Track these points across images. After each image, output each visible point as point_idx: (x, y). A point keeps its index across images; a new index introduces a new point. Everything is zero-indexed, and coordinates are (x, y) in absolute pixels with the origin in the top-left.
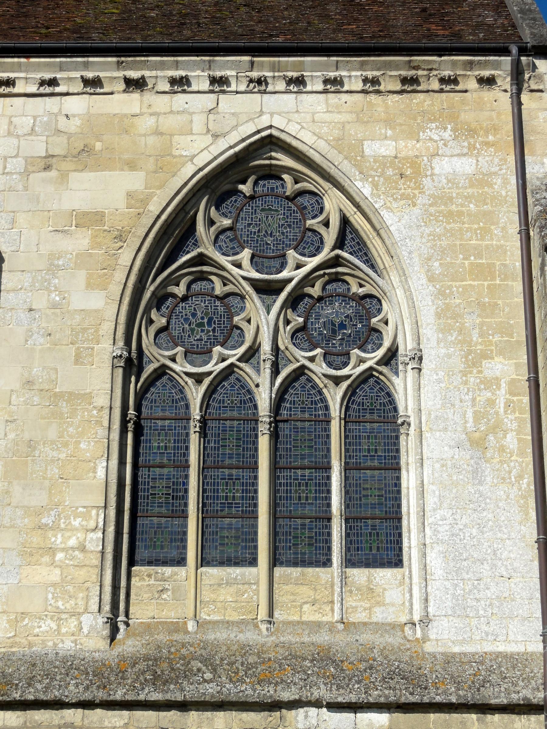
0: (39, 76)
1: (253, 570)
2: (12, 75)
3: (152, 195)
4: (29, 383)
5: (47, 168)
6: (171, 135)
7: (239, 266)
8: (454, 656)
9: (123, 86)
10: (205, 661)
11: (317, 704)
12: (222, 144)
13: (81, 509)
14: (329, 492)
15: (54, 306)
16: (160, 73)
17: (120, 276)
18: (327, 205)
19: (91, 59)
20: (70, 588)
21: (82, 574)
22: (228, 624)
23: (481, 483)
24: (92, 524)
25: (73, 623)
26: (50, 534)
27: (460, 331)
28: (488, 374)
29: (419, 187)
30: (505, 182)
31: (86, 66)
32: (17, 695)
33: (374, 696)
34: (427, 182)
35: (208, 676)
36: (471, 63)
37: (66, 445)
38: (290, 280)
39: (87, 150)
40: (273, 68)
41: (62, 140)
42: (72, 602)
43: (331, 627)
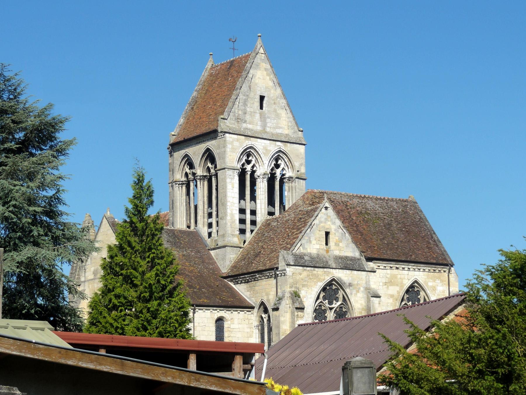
5: (385, 285)
18: (421, 293)
29: (435, 292)
30: (447, 292)
34: (436, 291)
41: (387, 279)
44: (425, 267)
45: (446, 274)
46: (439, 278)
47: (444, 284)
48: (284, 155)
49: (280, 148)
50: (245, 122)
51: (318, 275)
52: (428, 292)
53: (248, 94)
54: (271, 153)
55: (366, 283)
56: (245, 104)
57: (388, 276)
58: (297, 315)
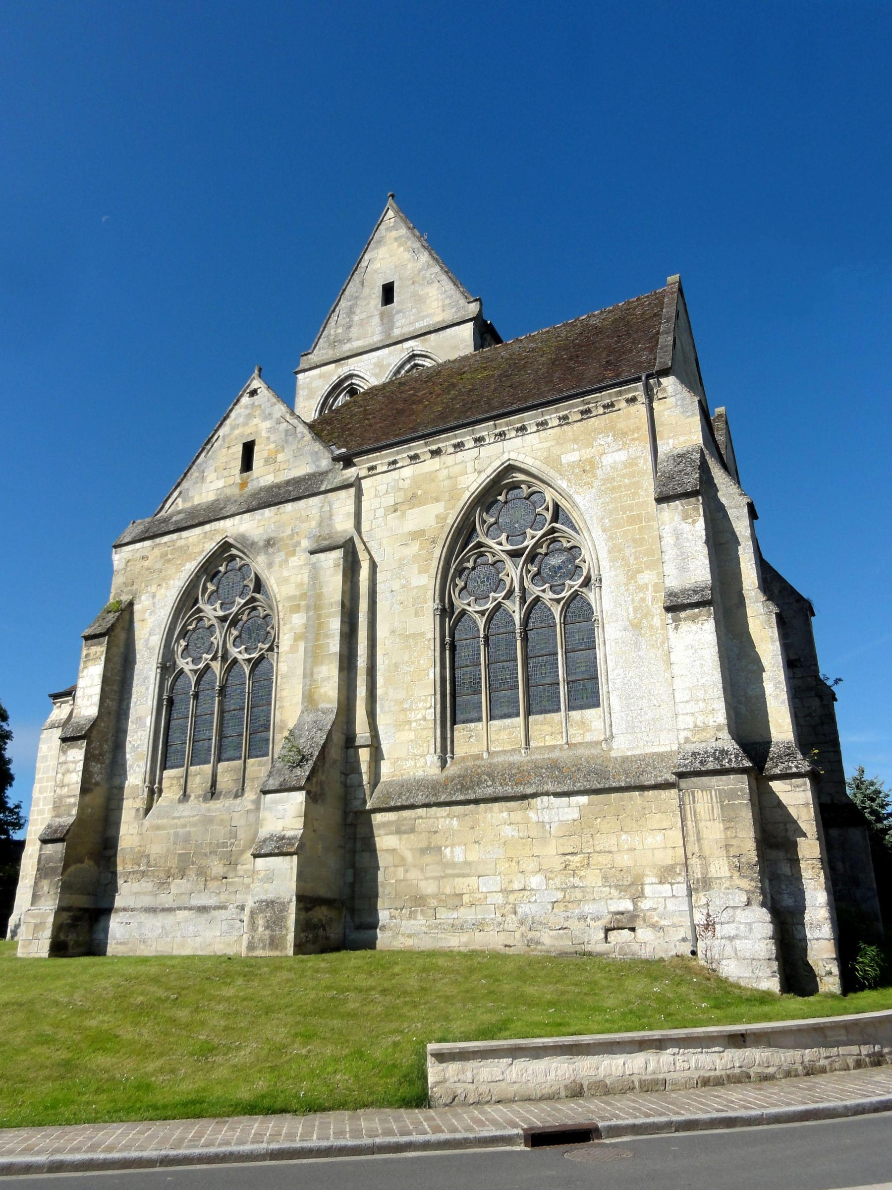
0: (387, 461)
1: (517, 719)
2: (374, 463)
3: (447, 515)
4: (393, 632)
5: (395, 511)
6: (456, 477)
7: (501, 544)
8: (627, 757)
9: (430, 455)
10: (489, 775)
11: (547, 794)
12: (483, 476)
13: (423, 697)
14: (557, 667)
15: (403, 587)
16: (448, 443)
17: (435, 563)
19: (411, 445)
20: (420, 742)
21: (425, 733)
22: (505, 752)
23: (639, 650)
24: (428, 705)
25: (422, 760)
26: (408, 713)
27: (623, 559)
28: (641, 582)
29: (594, 476)
30: (646, 461)
31: (410, 449)
32: (392, 804)
33: (578, 786)
34: (599, 472)
35: (489, 783)
36: (620, 391)
37: (413, 663)
38: (527, 547)
39: (414, 496)
40: (507, 424)
41: (402, 493)
42: (421, 749)
43: (561, 747)
44: (543, 414)
45: (640, 409)
46: (611, 428)
47: (634, 439)
48: (427, 359)
49: (413, 351)
50: (349, 340)
51: (188, 547)
52: (563, 484)
53: (357, 294)
54: (391, 369)
55: (320, 524)
56: (351, 312)
57: (406, 484)
58: (87, 656)
